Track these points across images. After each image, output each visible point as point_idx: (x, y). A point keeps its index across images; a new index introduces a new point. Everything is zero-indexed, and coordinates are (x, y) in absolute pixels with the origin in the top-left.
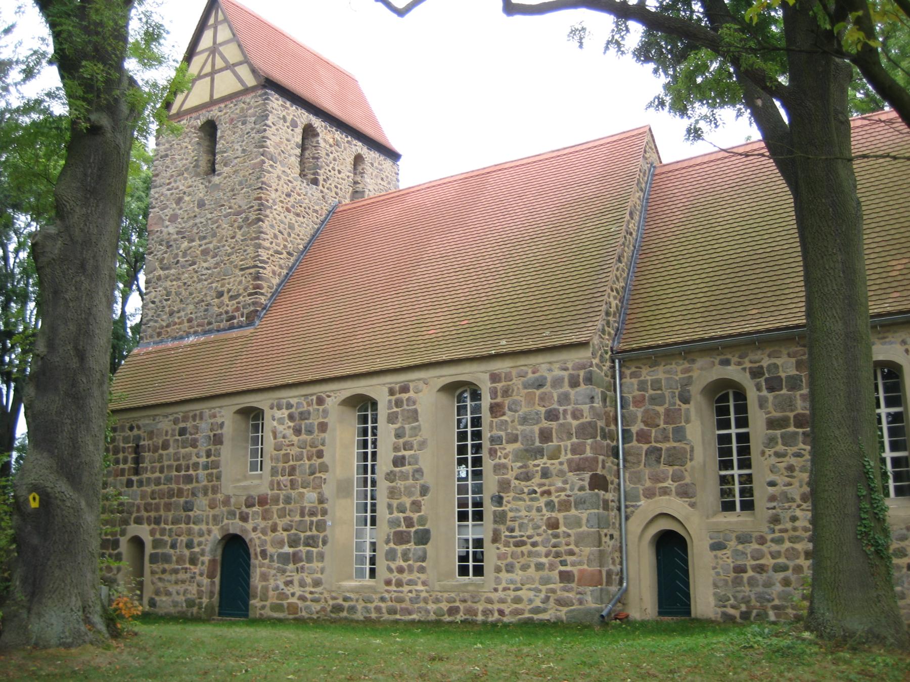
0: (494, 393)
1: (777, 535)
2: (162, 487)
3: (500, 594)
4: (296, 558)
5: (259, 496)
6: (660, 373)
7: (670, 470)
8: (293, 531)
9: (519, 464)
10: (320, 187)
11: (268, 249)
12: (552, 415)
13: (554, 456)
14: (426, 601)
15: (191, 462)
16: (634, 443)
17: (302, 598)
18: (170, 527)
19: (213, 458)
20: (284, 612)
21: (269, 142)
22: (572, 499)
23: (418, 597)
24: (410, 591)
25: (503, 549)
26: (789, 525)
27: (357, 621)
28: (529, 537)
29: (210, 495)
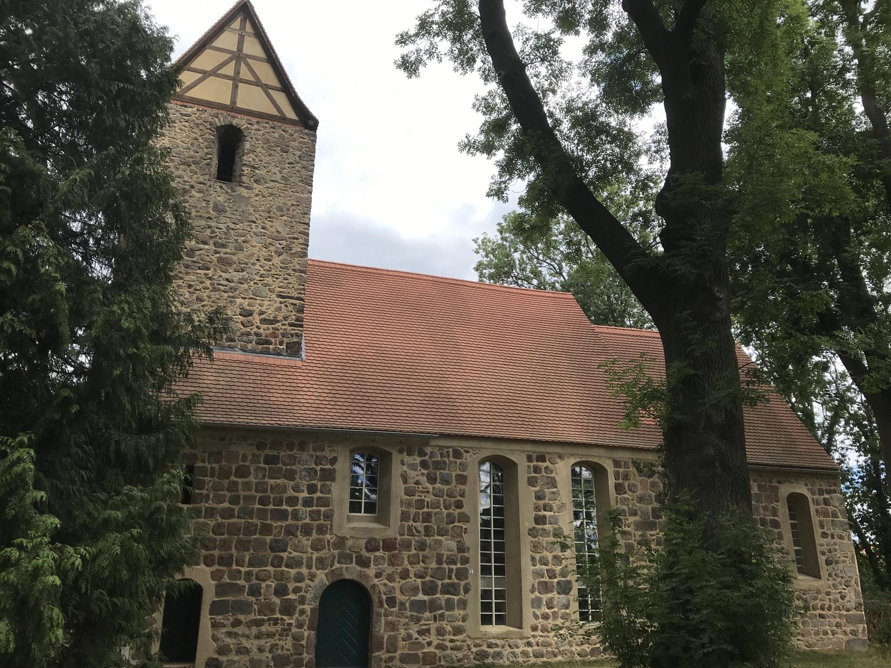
0: (617, 475)
2: (235, 520)
4: (433, 606)
5: (383, 541)
8: (428, 578)
9: (640, 533)
15: (285, 496)
18: (247, 569)
19: (319, 494)
29: (315, 536)
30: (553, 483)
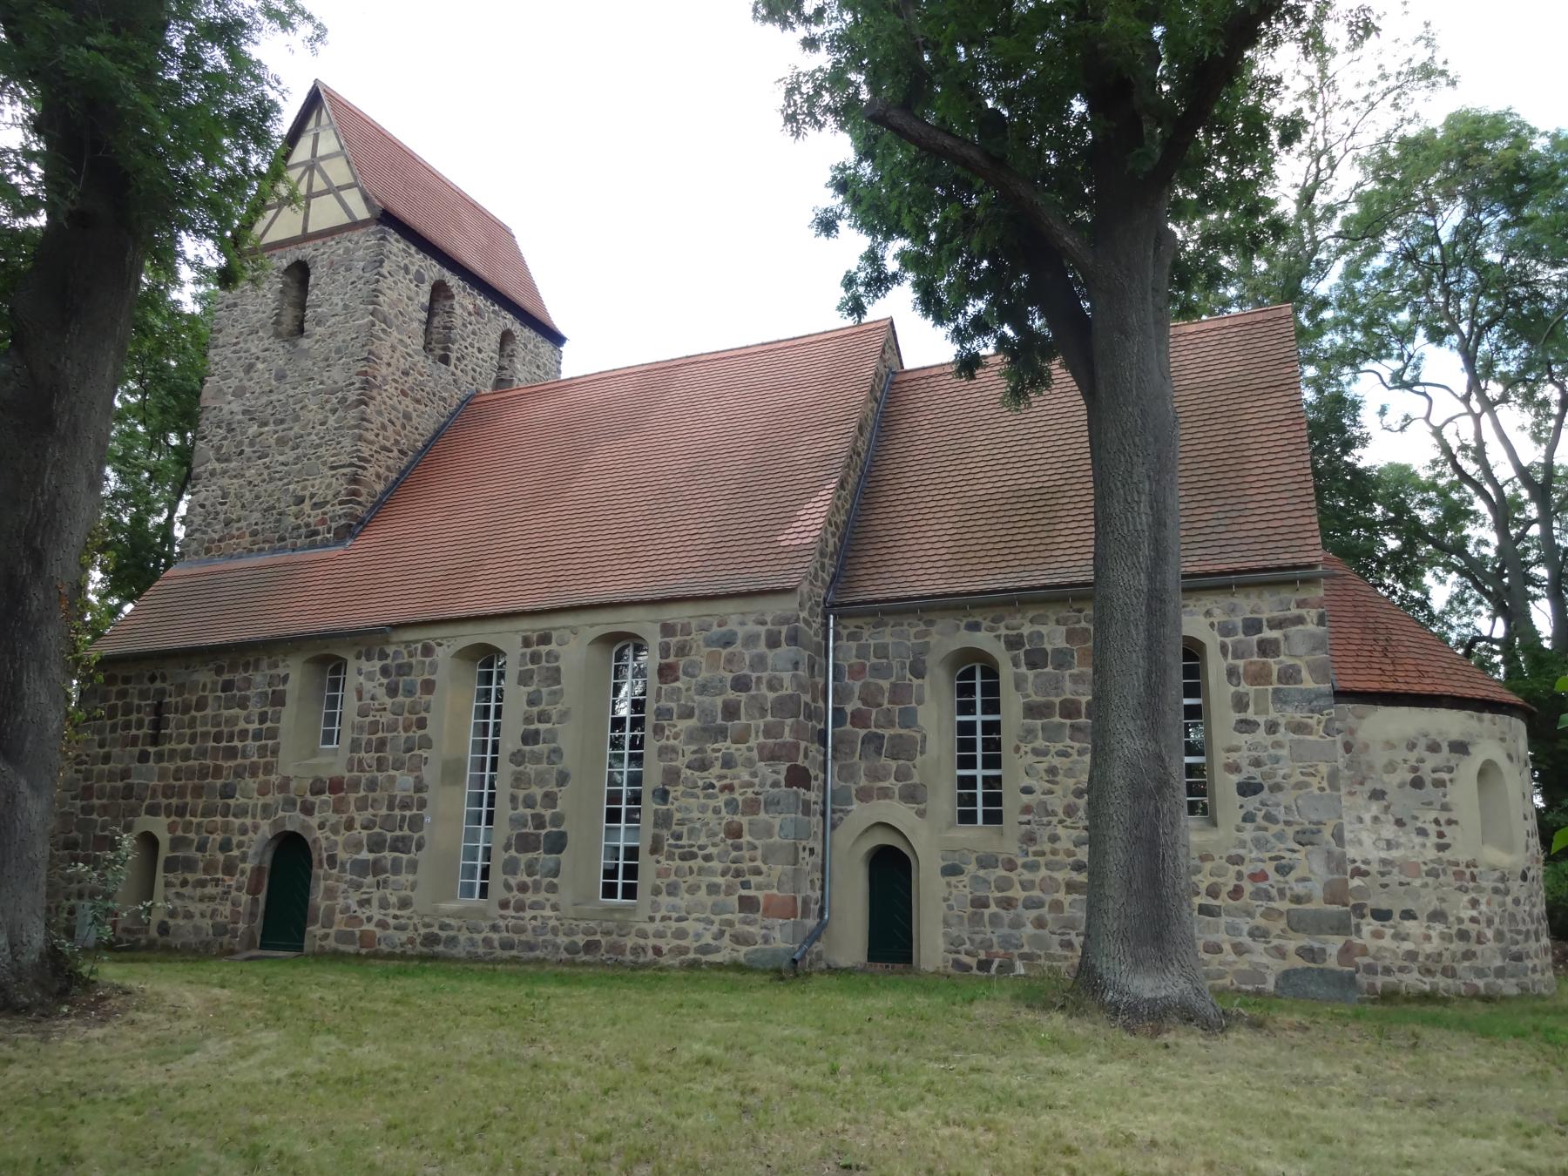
0: (665, 650)
1: (1031, 858)
3: (658, 925)
4: (376, 868)
6: (887, 637)
7: (893, 765)
8: (377, 830)
9: (693, 748)
10: (452, 368)
11: (372, 443)
12: (741, 684)
13: (741, 738)
14: (555, 931)
15: (237, 729)
16: (848, 727)
17: (382, 924)
18: (199, 819)
19: (268, 724)
20: (353, 943)
21: (381, 298)
22: (761, 798)
23: (544, 925)
24: (534, 918)
25: (665, 863)
26: (1047, 847)
27: (457, 960)
28: (701, 848)
30: (554, 676)
